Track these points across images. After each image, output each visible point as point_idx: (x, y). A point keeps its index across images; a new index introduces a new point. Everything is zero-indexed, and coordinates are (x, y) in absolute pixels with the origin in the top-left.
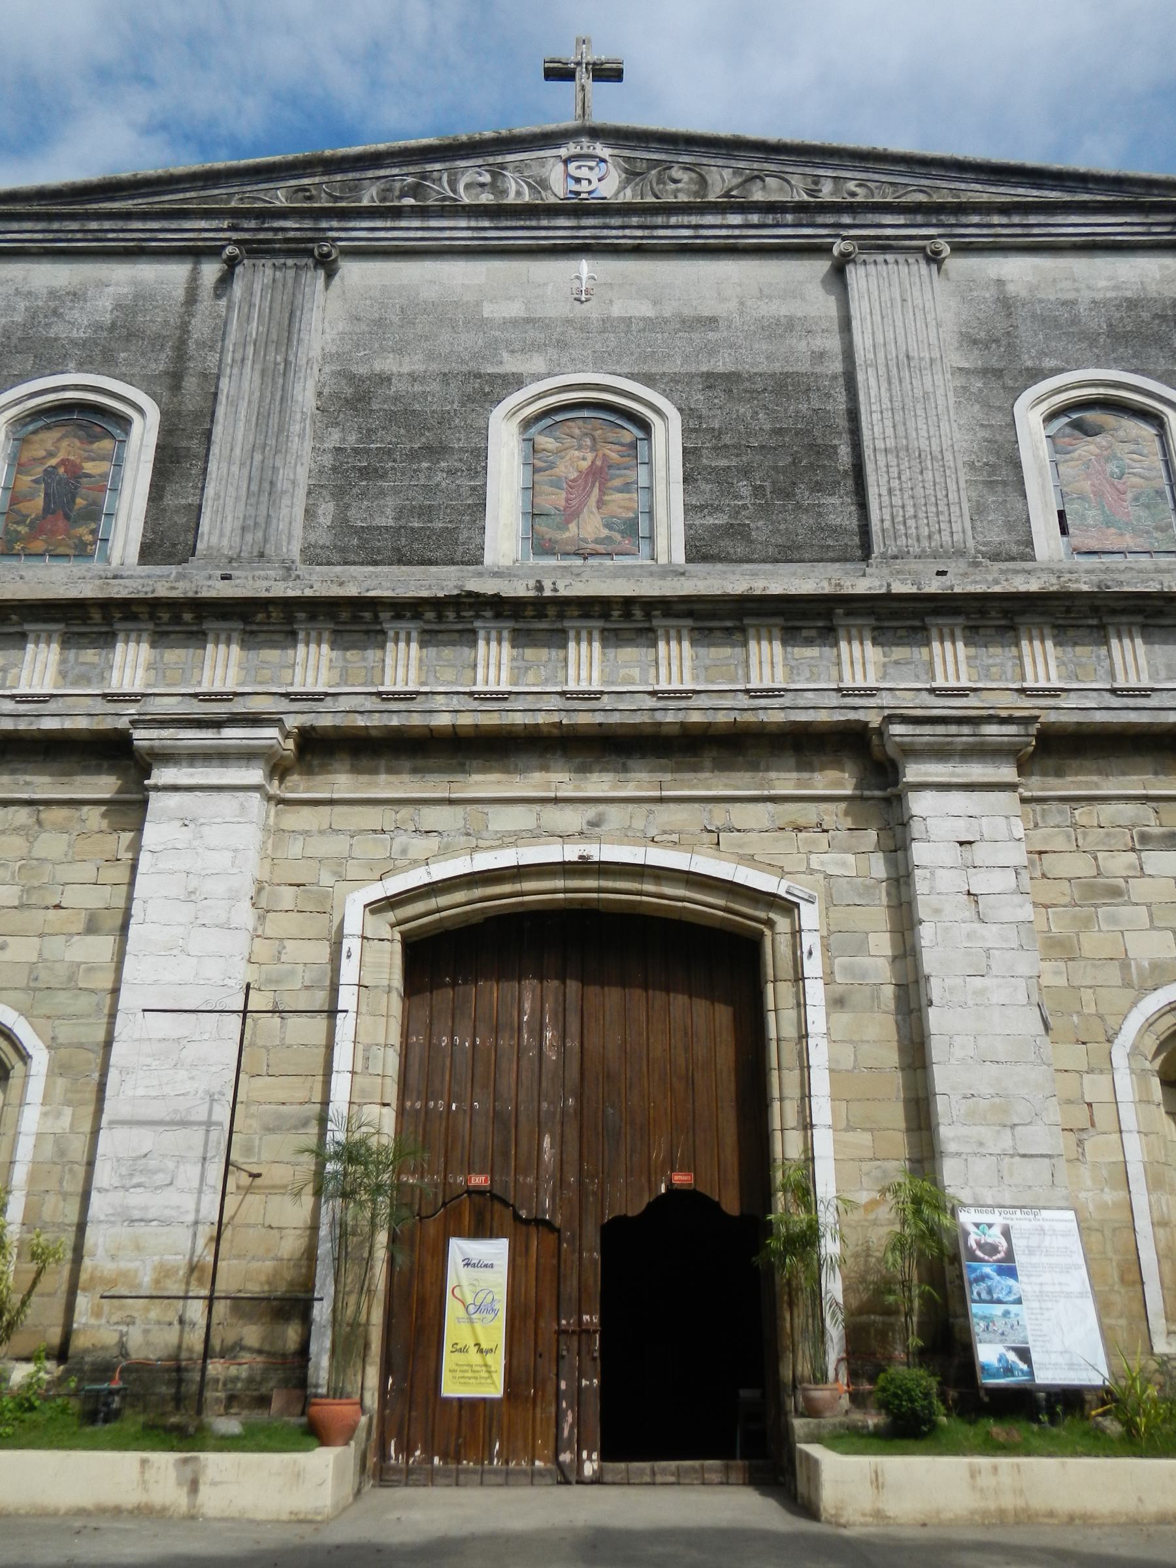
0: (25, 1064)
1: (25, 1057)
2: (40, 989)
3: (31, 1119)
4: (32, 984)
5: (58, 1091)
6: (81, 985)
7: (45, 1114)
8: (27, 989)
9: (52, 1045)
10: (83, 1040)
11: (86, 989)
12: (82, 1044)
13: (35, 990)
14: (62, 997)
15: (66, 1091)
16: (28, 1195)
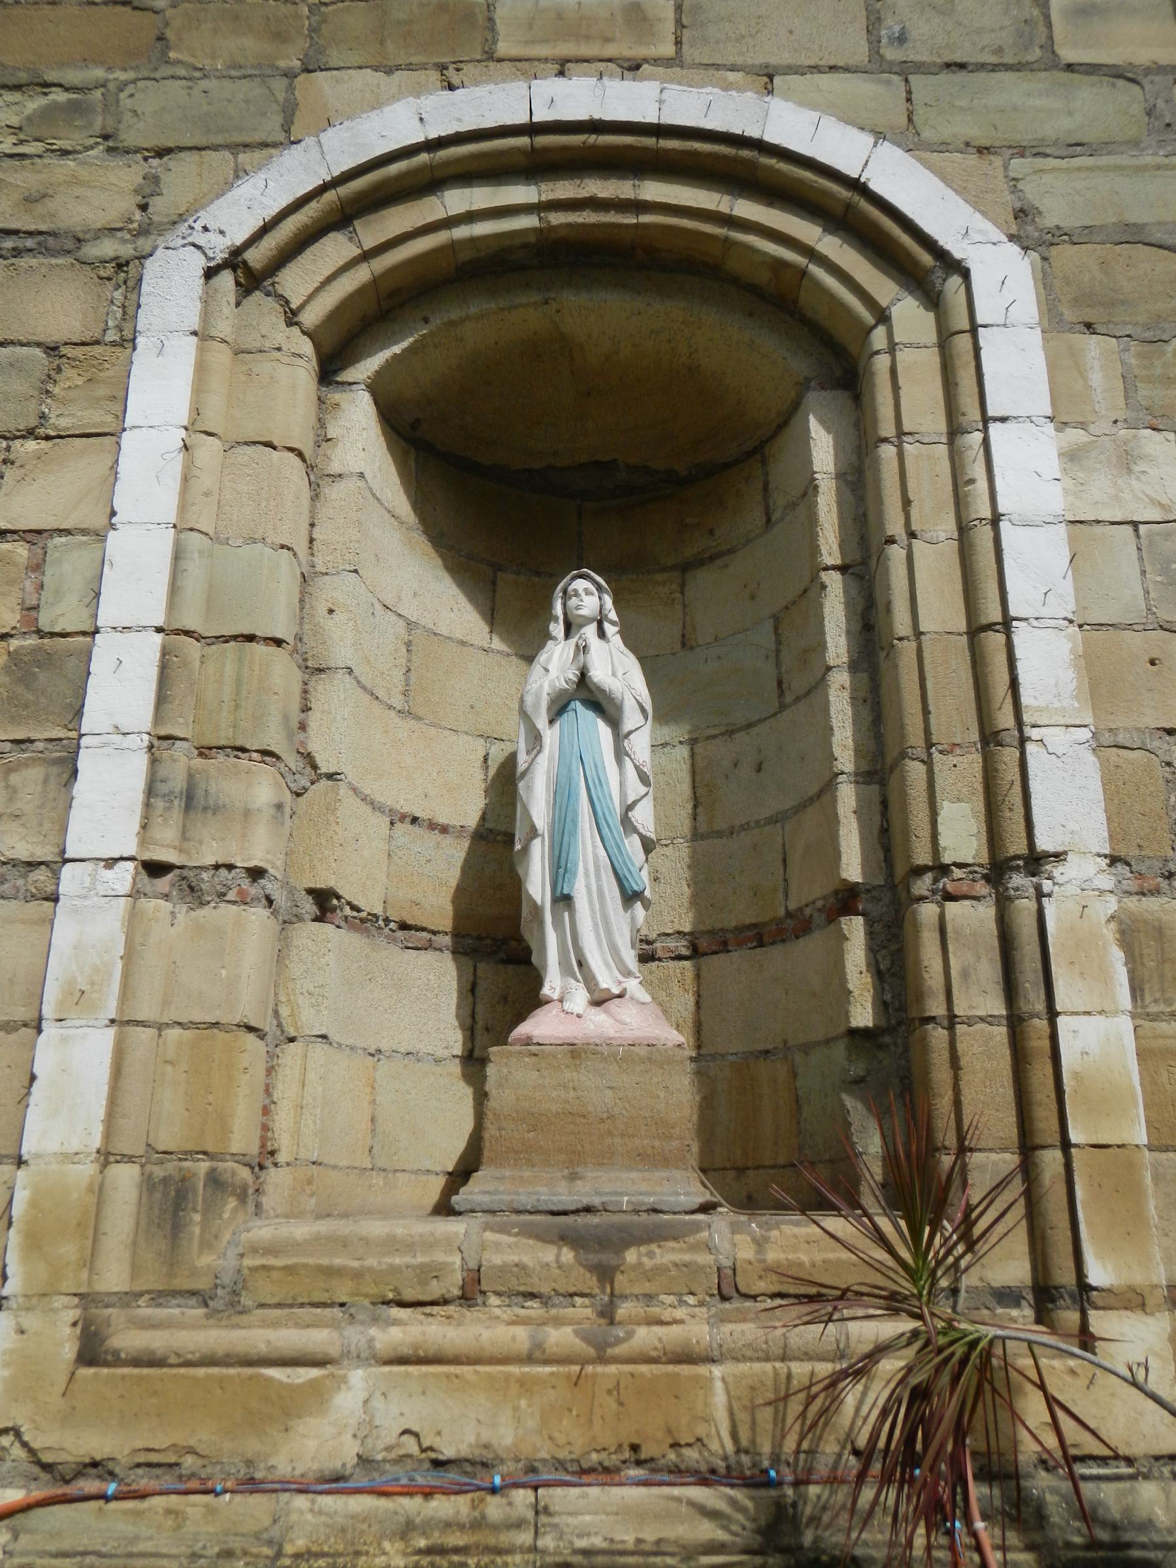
0: (933, 300)
1: (927, 269)
2: (921, 68)
3: (1027, 468)
4: (891, 54)
5: (1096, 378)
6: (1068, 54)
7: (1071, 456)
8: (876, 65)
9: (1024, 227)
10: (1134, 217)
11: (1092, 69)
12: (1140, 227)
13: (905, 70)
14: (1011, 90)
15: (1129, 382)
16: (1104, 744)
